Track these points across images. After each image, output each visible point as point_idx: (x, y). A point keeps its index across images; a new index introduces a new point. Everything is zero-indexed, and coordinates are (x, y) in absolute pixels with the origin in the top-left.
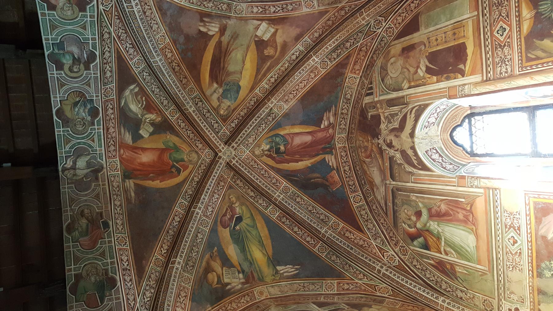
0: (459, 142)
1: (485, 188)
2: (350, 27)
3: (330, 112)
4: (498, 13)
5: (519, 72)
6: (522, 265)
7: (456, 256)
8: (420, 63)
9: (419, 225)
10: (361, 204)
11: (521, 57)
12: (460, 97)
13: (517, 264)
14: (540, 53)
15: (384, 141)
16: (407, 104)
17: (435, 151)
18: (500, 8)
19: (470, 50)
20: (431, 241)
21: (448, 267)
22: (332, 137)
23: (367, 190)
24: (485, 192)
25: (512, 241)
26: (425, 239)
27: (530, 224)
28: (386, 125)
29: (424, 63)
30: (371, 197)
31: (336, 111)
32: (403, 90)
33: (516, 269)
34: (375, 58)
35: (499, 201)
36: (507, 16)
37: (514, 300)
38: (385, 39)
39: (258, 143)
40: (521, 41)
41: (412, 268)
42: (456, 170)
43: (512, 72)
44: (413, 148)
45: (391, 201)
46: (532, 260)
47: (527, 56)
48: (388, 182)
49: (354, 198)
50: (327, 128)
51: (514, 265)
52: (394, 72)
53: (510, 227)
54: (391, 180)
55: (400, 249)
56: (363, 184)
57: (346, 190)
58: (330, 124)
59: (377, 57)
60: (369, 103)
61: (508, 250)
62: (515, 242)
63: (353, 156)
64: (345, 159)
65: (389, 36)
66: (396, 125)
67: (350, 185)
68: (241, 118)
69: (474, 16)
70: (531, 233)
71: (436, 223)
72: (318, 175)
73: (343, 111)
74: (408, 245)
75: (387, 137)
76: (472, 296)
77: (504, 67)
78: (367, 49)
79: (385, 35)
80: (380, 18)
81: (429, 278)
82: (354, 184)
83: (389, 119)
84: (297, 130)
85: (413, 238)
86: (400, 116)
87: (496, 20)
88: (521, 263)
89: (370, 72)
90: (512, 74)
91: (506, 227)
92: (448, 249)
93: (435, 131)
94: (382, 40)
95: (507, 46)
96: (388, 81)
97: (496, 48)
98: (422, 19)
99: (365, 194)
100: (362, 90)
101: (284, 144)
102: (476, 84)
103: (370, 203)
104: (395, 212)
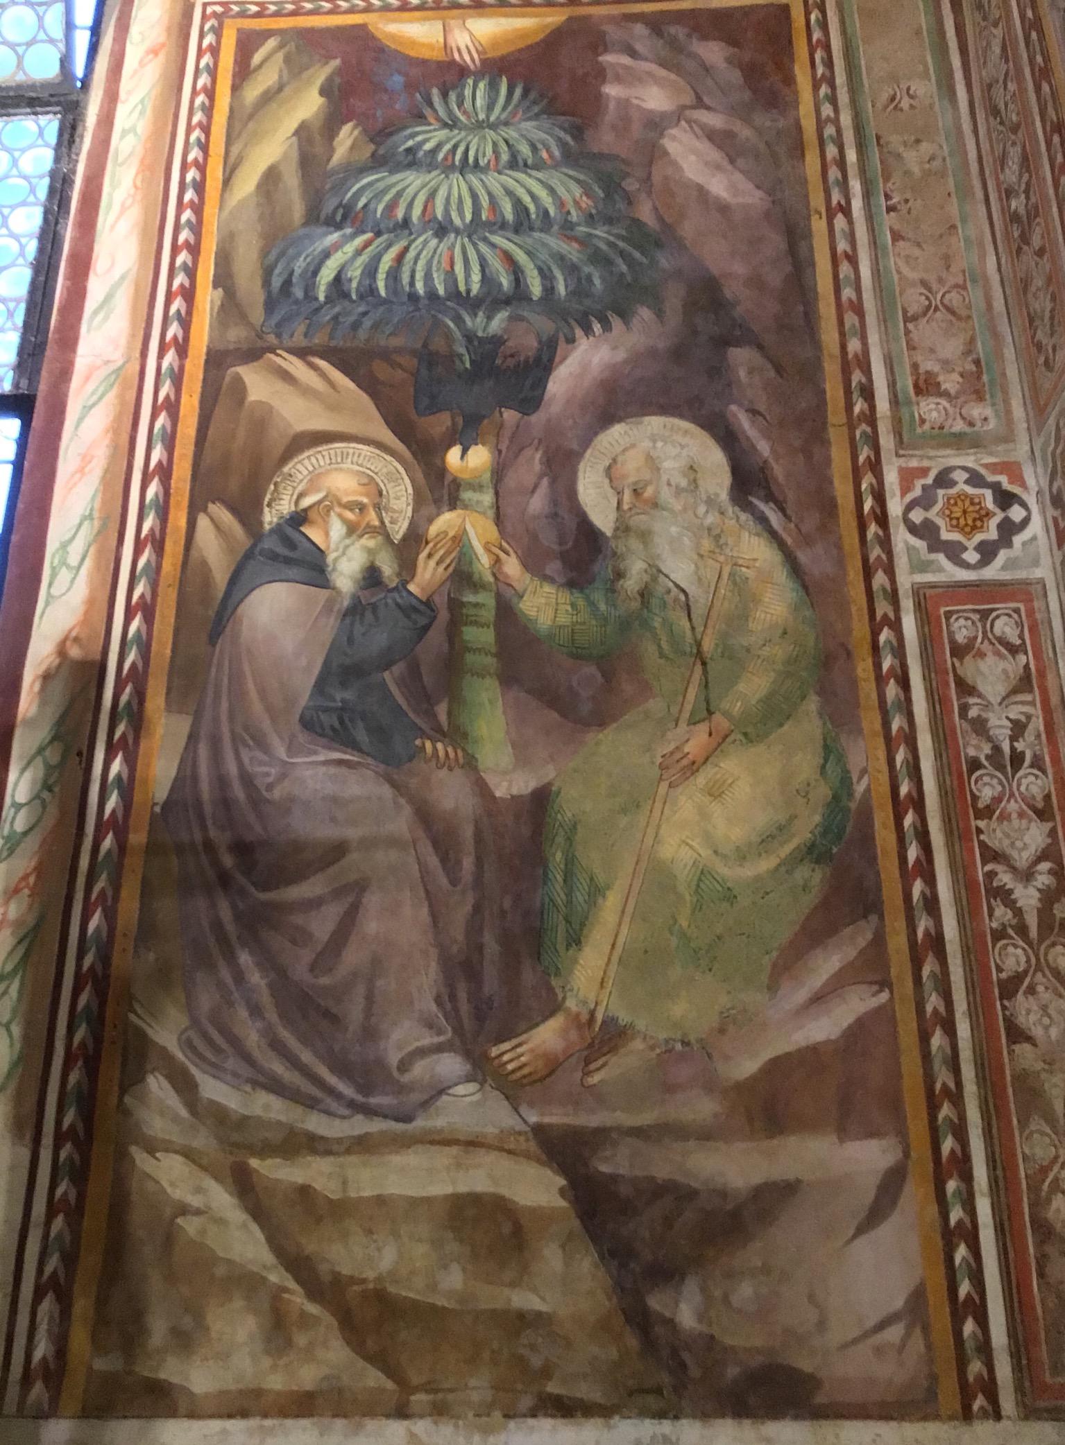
14: (266, 79)
47: (267, 34)
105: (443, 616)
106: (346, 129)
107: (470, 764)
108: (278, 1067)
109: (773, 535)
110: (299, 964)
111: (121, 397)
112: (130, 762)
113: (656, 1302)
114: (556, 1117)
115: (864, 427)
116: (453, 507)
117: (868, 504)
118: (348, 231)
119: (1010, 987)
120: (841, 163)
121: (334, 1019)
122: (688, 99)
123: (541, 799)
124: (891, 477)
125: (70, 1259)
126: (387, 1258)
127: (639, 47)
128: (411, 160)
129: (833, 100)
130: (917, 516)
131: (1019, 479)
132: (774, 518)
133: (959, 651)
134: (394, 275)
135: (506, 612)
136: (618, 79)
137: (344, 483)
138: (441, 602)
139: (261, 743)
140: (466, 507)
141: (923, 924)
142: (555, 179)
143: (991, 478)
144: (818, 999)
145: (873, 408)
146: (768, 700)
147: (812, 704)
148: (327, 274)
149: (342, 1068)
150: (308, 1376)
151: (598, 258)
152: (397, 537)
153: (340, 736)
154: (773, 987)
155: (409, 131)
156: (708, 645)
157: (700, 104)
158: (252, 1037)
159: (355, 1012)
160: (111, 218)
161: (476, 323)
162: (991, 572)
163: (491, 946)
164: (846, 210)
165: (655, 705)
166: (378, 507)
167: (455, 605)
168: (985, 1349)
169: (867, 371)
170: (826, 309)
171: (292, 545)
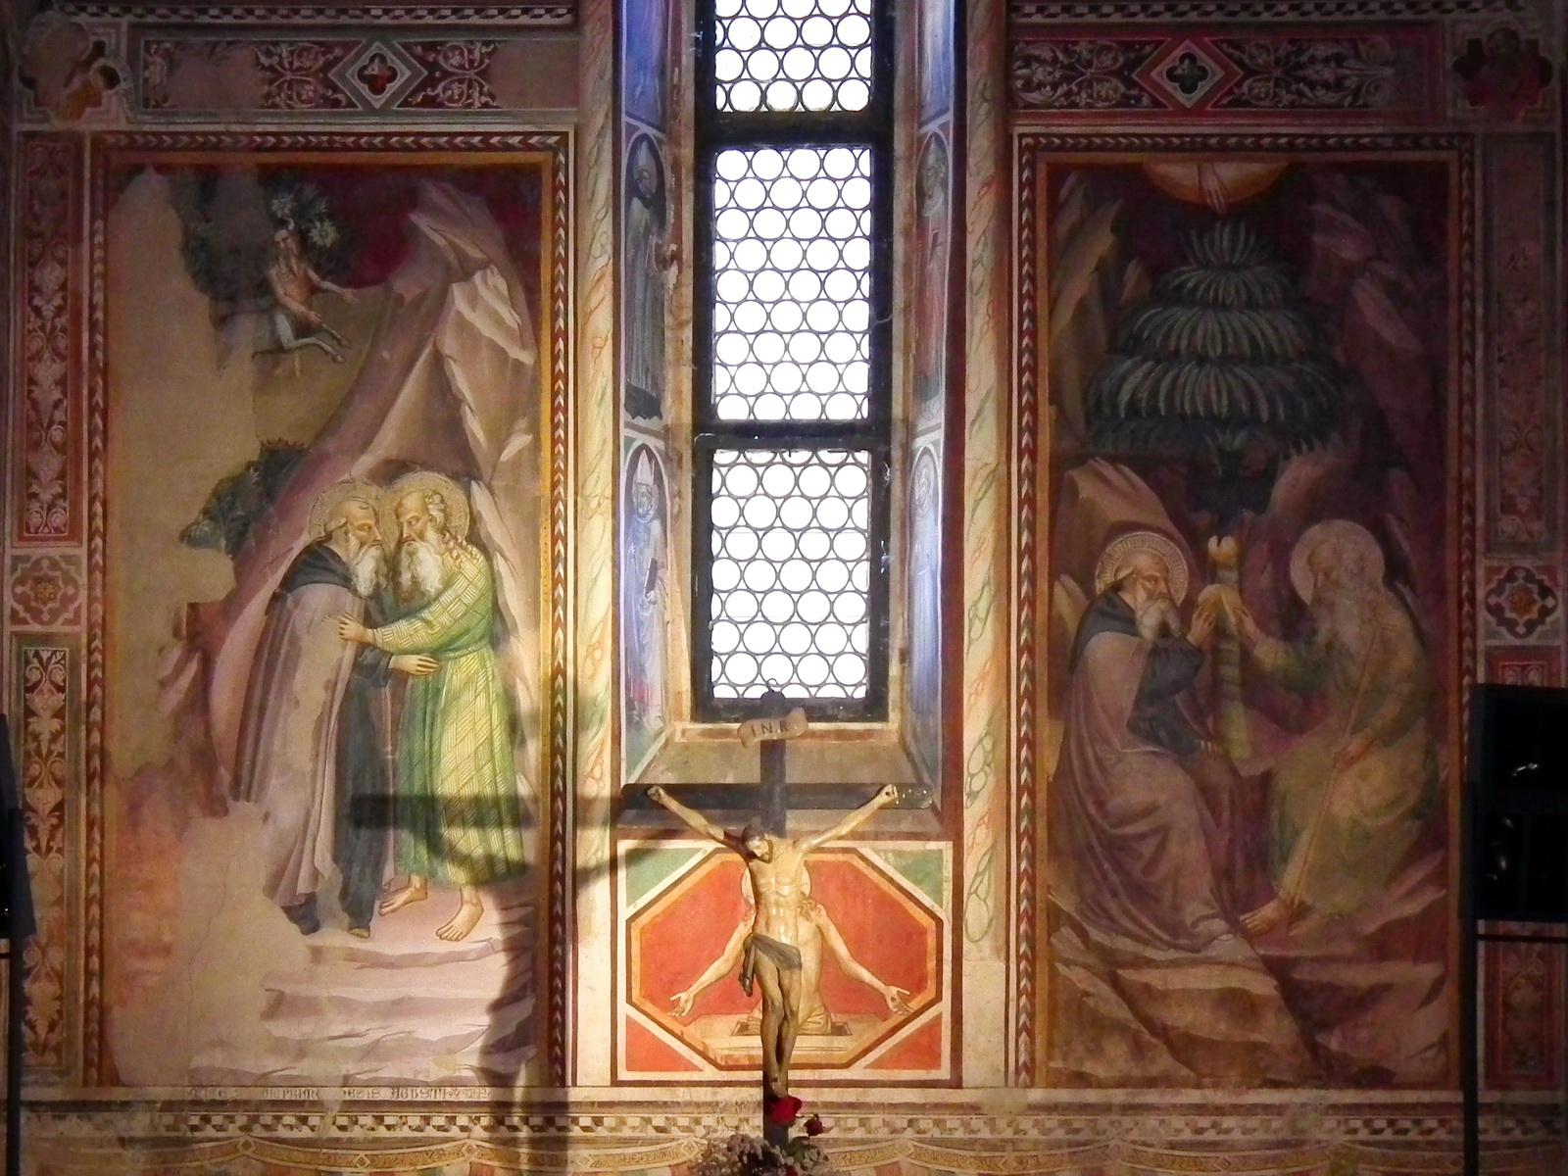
4: (1260, 61)
5: (1021, 136)
6: (290, 107)
11: (1075, 148)
13: (290, 88)
25: (375, 69)
27: (456, 148)
33: (271, 82)
36: (1237, 102)
37: (146, 67)
40: (1130, 148)
43: (1025, 107)
46: (318, 148)
51: (282, 75)
53: (433, 66)
61: (338, 52)
62: (377, 85)
70: (421, 148)
77: (1050, 73)
87: (1237, 53)
88: (300, 107)
90: (1015, 106)
91: (430, 47)
95: (1124, 95)
97: (1128, 46)
105: (1209, 658)
106: (1132, 265)
108: (1129, 925)
109: (1407, 606)
110: (1137, 869)
111: (998, 492)
113: (1320, 1039)
114: (1274, 951)
115: (1467, 536)
116: (1213, 582)
117: (1465, 591)
118: (1138, 358)
120: (1472, 317)
121: (1157, 900)
123: (1267, 779)
124: (1480, 573)
125: (1032, 1016)
128: (1178, 297)
130: (1493, 600)
132: (1409, 599)
135: (1246, 654)
137: (1144, 562)
138: (1207, 648)
139: (1106, 741)
140: (1220, 582)
143: (1538, 577)
145: (1474, 520)
147: (1421, 722)
148: (1124, 397)
149: (1162, 926)
150: (1154, 1070)
152: (1179, 603)
153: (1151, 737)
154: (1387, 887)
155: (1175, 271)
158: (1113, 908)
159: (1167, 896)
160: (976, 339)
162: (1531, 641)
163: (1240, 863)
164: (1471, 358)
166: (1166, 581)
167: (1216, 651)
169: (1473, 494)
170: (1452, 441)
171: (1115, 606)
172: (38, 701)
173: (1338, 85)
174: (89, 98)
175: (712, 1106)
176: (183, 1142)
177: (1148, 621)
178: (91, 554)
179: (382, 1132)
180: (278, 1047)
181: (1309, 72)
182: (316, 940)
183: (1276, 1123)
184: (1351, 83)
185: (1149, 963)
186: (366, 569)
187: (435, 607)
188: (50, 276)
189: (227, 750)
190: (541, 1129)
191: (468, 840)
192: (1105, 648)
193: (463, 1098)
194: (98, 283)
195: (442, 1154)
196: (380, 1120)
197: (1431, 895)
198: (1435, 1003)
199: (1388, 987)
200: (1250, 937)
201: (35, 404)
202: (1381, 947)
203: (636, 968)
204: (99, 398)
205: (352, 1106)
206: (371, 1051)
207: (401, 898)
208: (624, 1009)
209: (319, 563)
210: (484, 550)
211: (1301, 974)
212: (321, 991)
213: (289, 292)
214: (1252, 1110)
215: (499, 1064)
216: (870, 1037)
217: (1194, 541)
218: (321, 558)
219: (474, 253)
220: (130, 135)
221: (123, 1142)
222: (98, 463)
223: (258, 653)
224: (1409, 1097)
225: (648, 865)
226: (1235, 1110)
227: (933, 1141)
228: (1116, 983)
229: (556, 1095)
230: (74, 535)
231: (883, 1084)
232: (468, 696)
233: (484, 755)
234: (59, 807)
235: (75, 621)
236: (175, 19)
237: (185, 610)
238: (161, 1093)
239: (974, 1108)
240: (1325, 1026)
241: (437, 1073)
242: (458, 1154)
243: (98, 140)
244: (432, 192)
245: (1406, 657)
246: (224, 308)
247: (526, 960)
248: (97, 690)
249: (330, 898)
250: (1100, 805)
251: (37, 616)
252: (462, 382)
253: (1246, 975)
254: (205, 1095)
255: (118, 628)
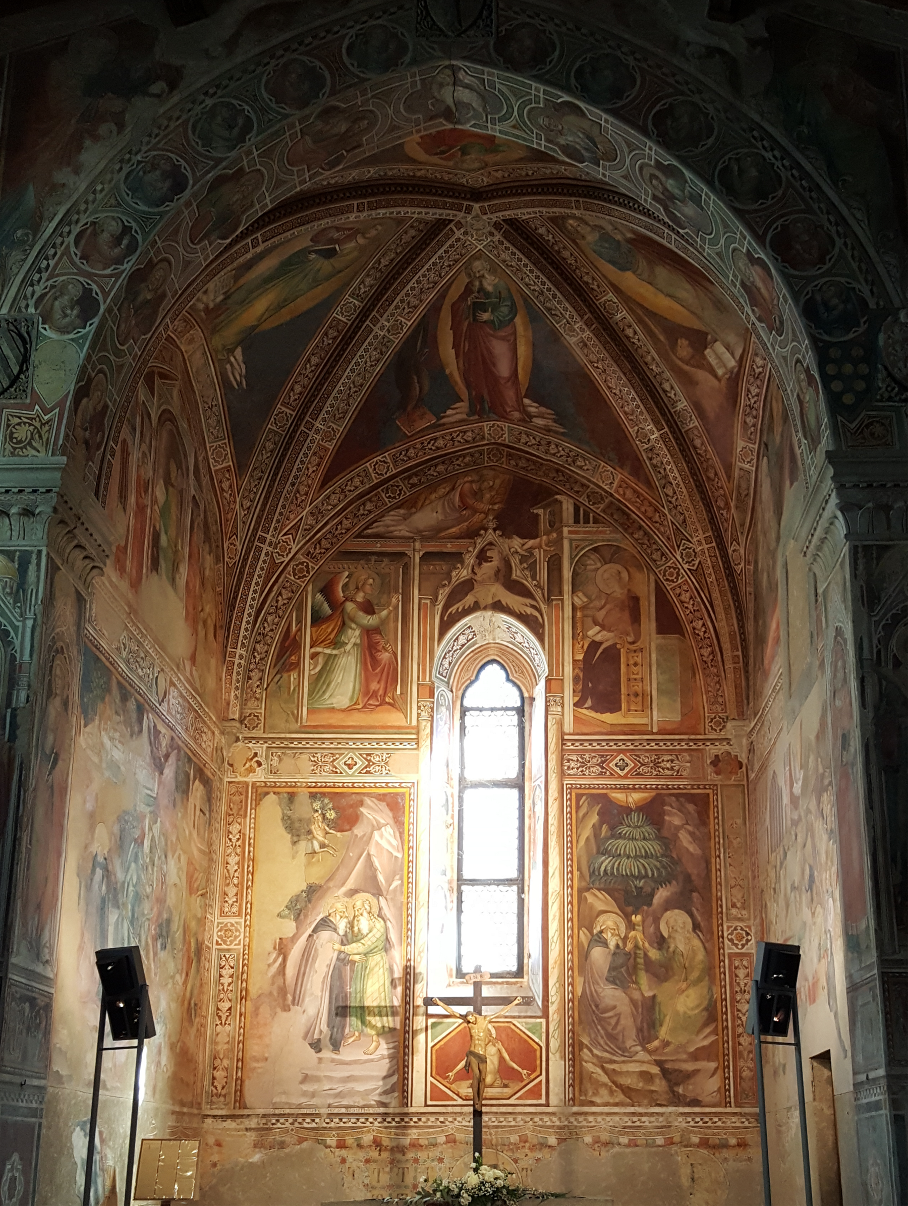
0: (483, 674)
1: (418, 728)
2: (694, 515)
3: (555, 422)
7: (312, 673)
8: (609, 631)
9: (350, 606)
10: (373, 475)
11: (585, 788)
12: (546, 697)
15: (491, 544)
16: (549, 601)
17: (470, 637)
18: (652, 765)
19: (609, 718)
20: (329, 628)
21: (293, 657)
22: (504, 417)
23: (400, 490)
24: (413, 728)
25: (350, 762)
26: (328, 618)
27: (376, 787)
28: (519, 550)
29: (605, 637)
30: (386, 500)
31: (556, 432)
32: (573, 593)
34: (636, 536)
35: (401, 746)
38: (662, 563)
39: (499, 270)
40: (603, 788)
41: (275, 588)
42: (442, 675)
44: (475, 607)
45: (384, 549)
46: (329, 787)
47: (583, 795)
48: (418, 545)
49: (384, 461)
50: (523, 409)
52: (606, 576)
53: (369, 761)
54: (421, 553)
55: (302, 563)
56: (411, 482)
57: (397, 445)
58: (531, 417)
59: (637, 540)
60: (561, 512)
62: (350, 767)
63: (464, 456)
64: (459, 438)
65: (665, 571)
66: (517, 574)
67: (407, 450)
68: (557, 248)
69: (652, 728)
70: (365, 787)
71: (358, 641)
72: (426, 388)
73: (553, 446)
74: (313, 580)
75: (496, 551)
76: (258, 696)
78: (656, 522)
79: (669, 564)
80: (697, 562)
81: (266, 620)
82: (410, 459)
83: (527, 558)
84: (523, 350)
85: (327, 591)
86: (529, 584)
88: (324, 773)
89: (616, 521)
91: (368, 755)
92: (321, 660)
93: (502, 637)
94: (663, 554)
96: (593, 562)
97: (602, 756)
98: (672, 640)
99: (391, 483)
100: (588, 497)
101: (493, 321)
102: (561, 724)
103: (376, 495)
104: (366, 555)
107: (640, 989)
108: (607, 1048)
110: (610, 1028)
112: (573, 987)
113: (676, 1089)
119: (739, 1036)
120: (719, 843)
121: (617, 1040)
122: (684, 822)
123: (654, 997)
125: (573, 1081)
126: (629, 1081)
127: (673, 805)
128: (620, 836)
129: (718, 824)
130: (730, 937)
131: (750, 929)
133: (736, 968)
134: (618, 869)
135: (646, 955)
136: (669, 815)
137: (610, 923)
138: (632, 953)
139: (598, 984)
141: (725, 1024)
142: (654, 843)
144: (705, 1037)
146: (699, 977)
147: (707, 978)
148: (603, 868)
149: (620, 1049)
150: (617, 1100)
151: (664, 867)
156: (687, 965)
157: (687, 824)
158: (602, 1042)
159: (621, 1037)
161: (637, 882)
162: (743, 951)
163: (645, 1025)
165: (676, 977)
167: (635, 953)
168: (730, 1096)
172: (224, 972)
173: (672, 769)
174: (251, 770)
175: (461, 1113)
176: (271, 1129)
177: (612, 944)
178: (245, 921)
179: (342, 1124)
180: (304, 1094)
181: (662, 764)
182: (320, 1055)
183: (661, 1119)
184: (676, 768)
185: (615, 1062)
186: (342, 926)
187: (366, 939)
188: (235, 828)
189: (290, 989)
190: (399, 1123)
191: (376, 1021)
192: (597, 953)
193: (371, 1112)
194: (252, 830)
195: (363, 1132)
196: (341, 1120)
197: (713, 1038)
198: (715, 1077)
199: (698, 1071)
200: (650, 1052)
201: (228, 871)
202: (695, 1056)
203: (434, 1064)
204: (251, 868)
205: (330, 1115)
206: (339, 1095)
207: (351, 1040)
208: (430, 1079)
209: (325, 923)
210: (383, 919)
211: (668, 1066)
212: (321, 1074)
213: (318, 834)
214: (652, 1114)
215: (384, 1099)
216: (517, 1088)
217: (627, 917)
218: (325, 922)
219: (382, 821)
220: (265, 782)
221: (247, 1129)
222: (249, 891)
223: (303, 955)
224: (707, 1110)
225: (439, 1028)
226: (646, 1114)
227: (539, 1126)
228: (603, 1068)
229: (405, 1110)
230: (239, 915)
231: (521, 1105)
232: (376, 969)
233: (382, 989)
234: (230, 1009)
235: (239, 944)
236: (282, 745)
237: (278, 940)
238: (261, 1111)
239: (554, 1114)
240: (678, 1084)
241: (362, 1103)
242: (369, 1132)
243: (254, 784)
244: (368, 801)
245: (701, 955)
246: (295, 839)
247: (395, 1061)
248: (245, 968)
249: (326, 1041)
250: (597, 1006)
251: (225, 942)
252: (377, 863)
253: (648, 1065)
254: (277, 1112)
255: (254, 945)
